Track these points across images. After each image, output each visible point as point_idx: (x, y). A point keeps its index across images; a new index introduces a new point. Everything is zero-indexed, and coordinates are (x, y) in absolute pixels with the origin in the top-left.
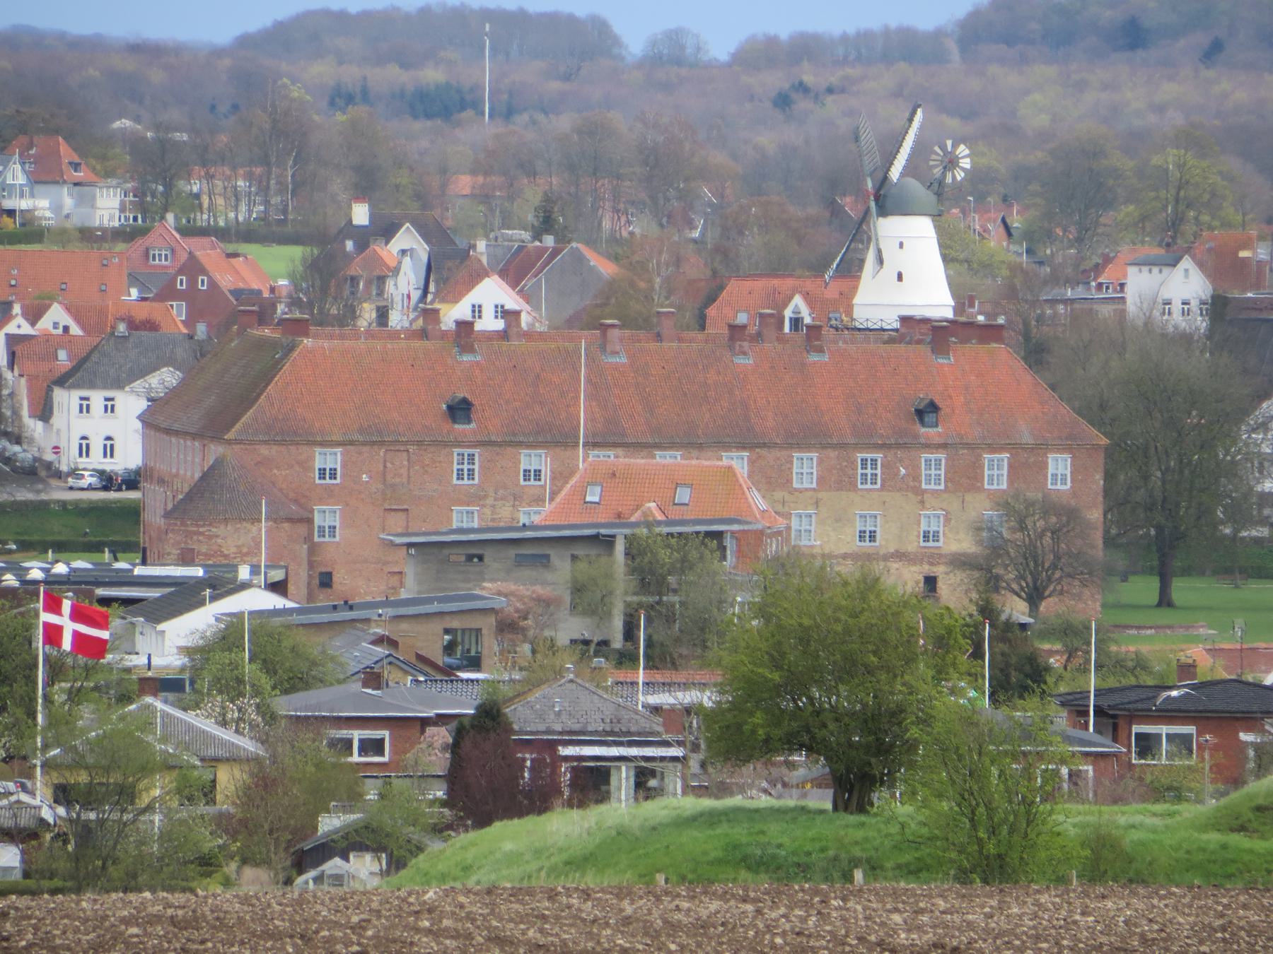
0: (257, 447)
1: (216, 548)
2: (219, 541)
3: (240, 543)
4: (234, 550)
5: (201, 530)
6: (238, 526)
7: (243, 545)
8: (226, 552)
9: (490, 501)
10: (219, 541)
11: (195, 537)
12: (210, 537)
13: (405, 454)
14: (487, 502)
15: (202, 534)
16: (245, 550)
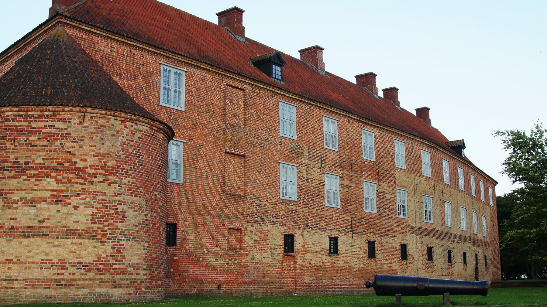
0: (96, 39)
1: (62, 156)
2: (68, 144)
3: (103, 150)
4: (92, 161)
5: (34, 125)
6: (102, 122)
7: (109, 155)
8: (81, 164)
9: (305, 160)
10: (68, 144)
11: (22, 138)
12: (50, 139)
13: (241, 93)
14: (303, 160)
15: (35, 131)
16: (111, 163)
